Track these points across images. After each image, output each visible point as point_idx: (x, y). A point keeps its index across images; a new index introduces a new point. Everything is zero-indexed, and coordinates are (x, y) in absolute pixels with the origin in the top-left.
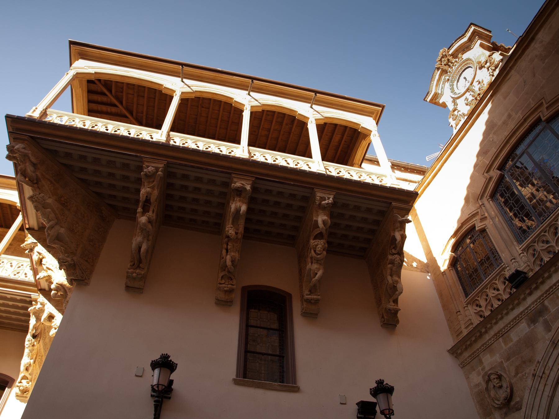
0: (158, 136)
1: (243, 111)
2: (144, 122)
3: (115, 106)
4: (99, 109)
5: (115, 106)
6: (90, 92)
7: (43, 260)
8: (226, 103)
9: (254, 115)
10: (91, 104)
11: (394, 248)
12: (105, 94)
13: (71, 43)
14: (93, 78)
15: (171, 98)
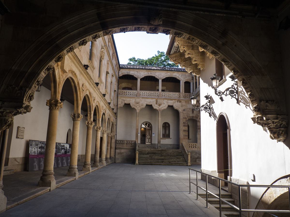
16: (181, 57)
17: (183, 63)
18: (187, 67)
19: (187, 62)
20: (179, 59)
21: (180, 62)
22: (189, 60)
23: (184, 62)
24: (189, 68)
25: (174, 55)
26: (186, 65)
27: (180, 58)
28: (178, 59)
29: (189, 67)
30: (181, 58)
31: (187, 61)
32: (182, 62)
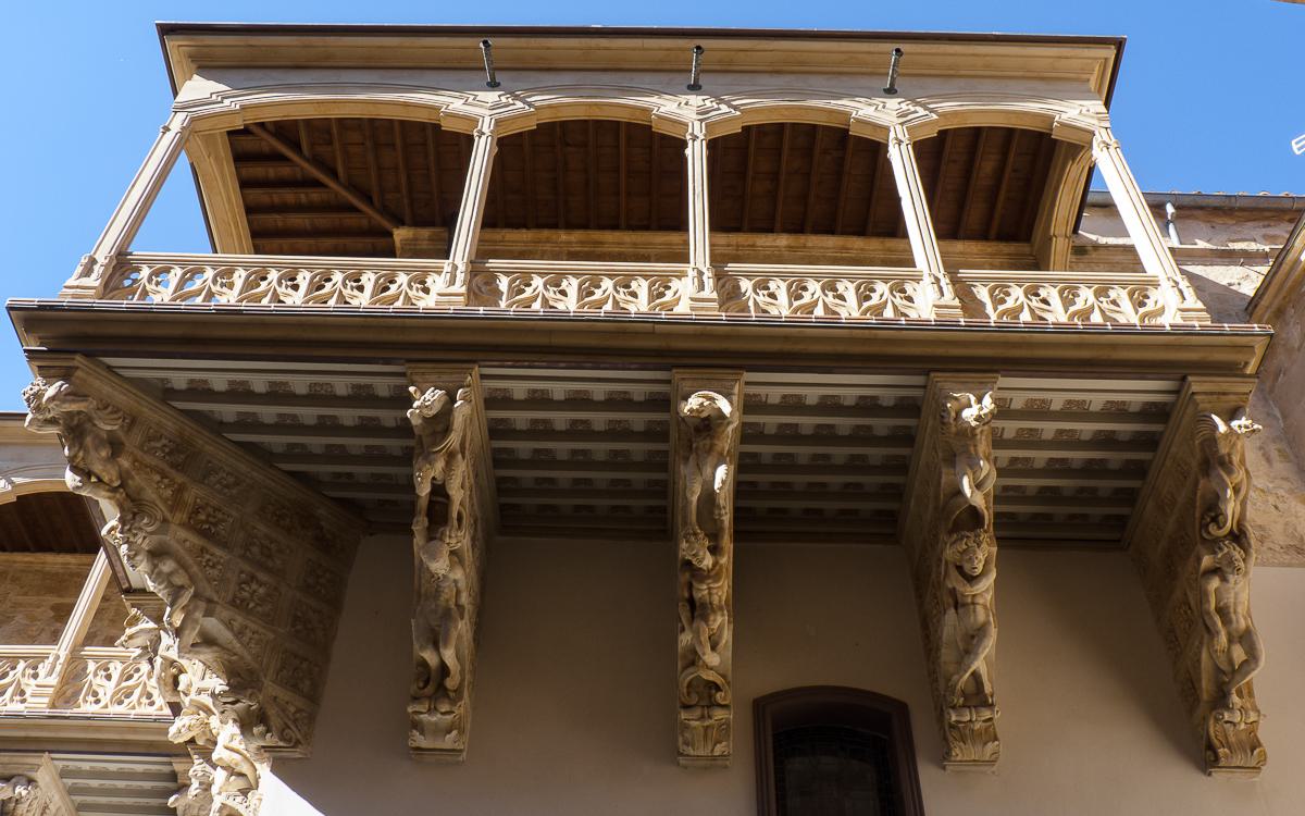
0: (438, 288)
1: (684, 144)
2: (407, 218)
3: (317, 184)
4: (276, 199)
5: (317, 184)
6: (240, 158)
7: (182, 678)
8: (630, 126)
9: (718, 149)
10: (248, 191)
11: (1215, 520)
12: (282, 158)
13: (166, 31)
14: (239, 124)
15: (470, 140)
16: (174, 466)
17: (183, 534)
18: (196, 596)
19: (218, 552)
20: (155, 469)
21: (150, 494)
22: (243, 557)
23: (195, 540)
24: (222, 621)
25: (121, 398)
26: (200, 563)
27: (167, 469)
28: (148, 459)
29: (226, 614)
30: (180, 478)
31: (224, 545)
32: (172, 509)
